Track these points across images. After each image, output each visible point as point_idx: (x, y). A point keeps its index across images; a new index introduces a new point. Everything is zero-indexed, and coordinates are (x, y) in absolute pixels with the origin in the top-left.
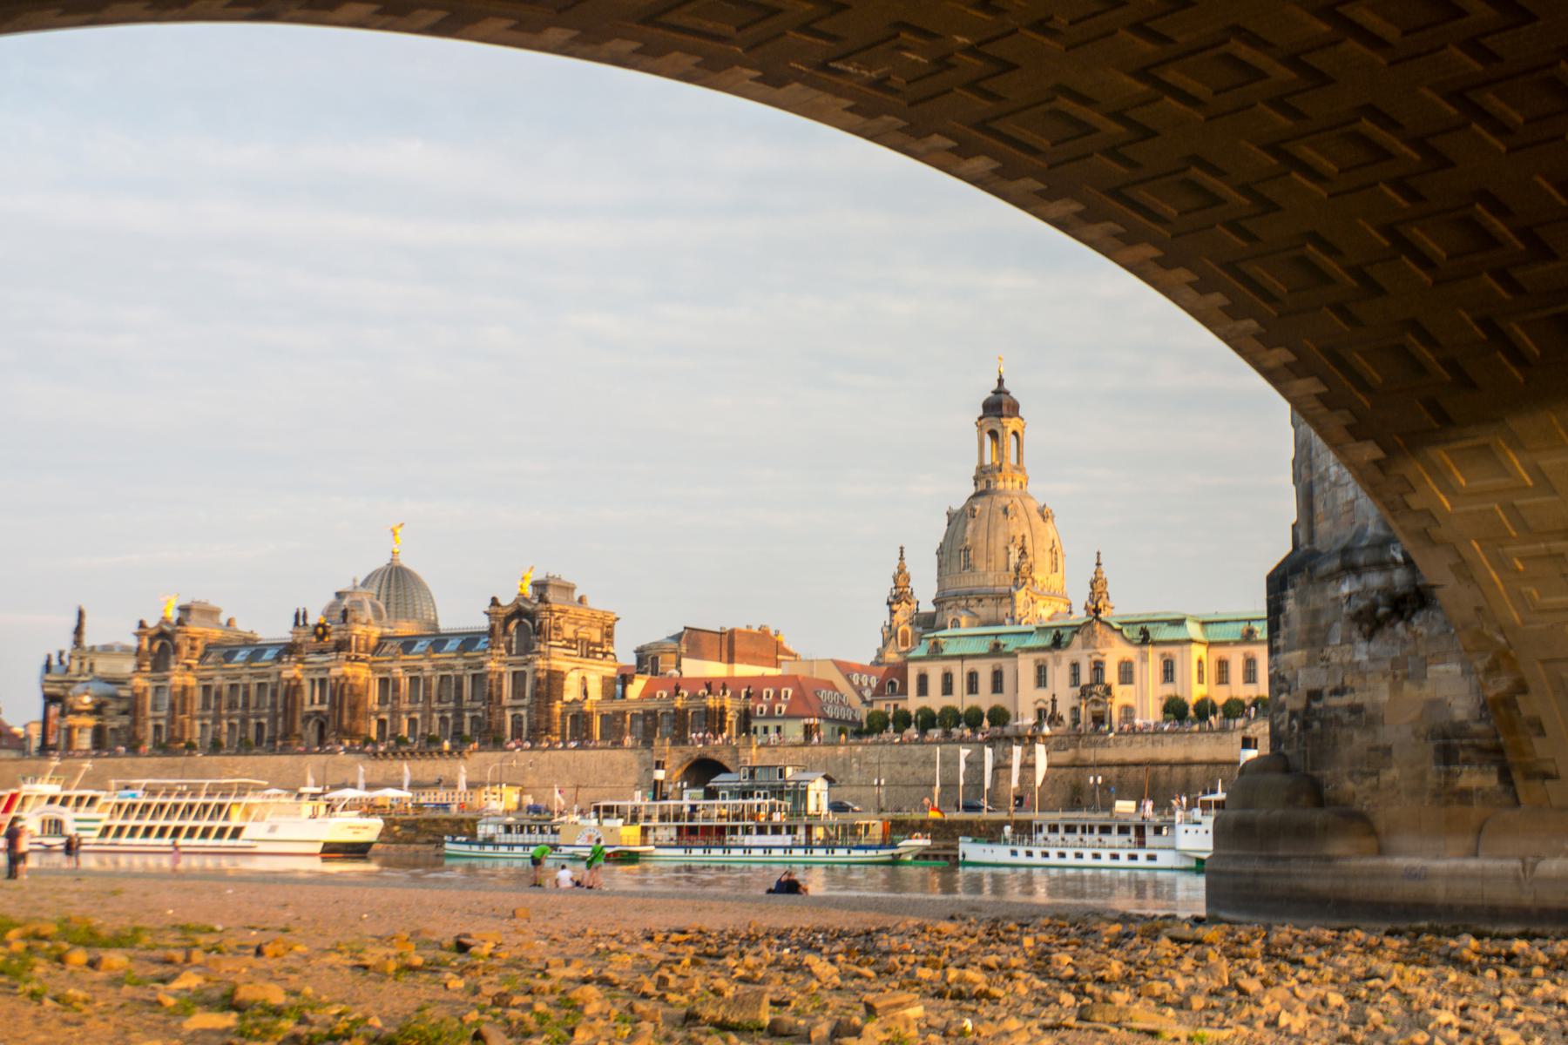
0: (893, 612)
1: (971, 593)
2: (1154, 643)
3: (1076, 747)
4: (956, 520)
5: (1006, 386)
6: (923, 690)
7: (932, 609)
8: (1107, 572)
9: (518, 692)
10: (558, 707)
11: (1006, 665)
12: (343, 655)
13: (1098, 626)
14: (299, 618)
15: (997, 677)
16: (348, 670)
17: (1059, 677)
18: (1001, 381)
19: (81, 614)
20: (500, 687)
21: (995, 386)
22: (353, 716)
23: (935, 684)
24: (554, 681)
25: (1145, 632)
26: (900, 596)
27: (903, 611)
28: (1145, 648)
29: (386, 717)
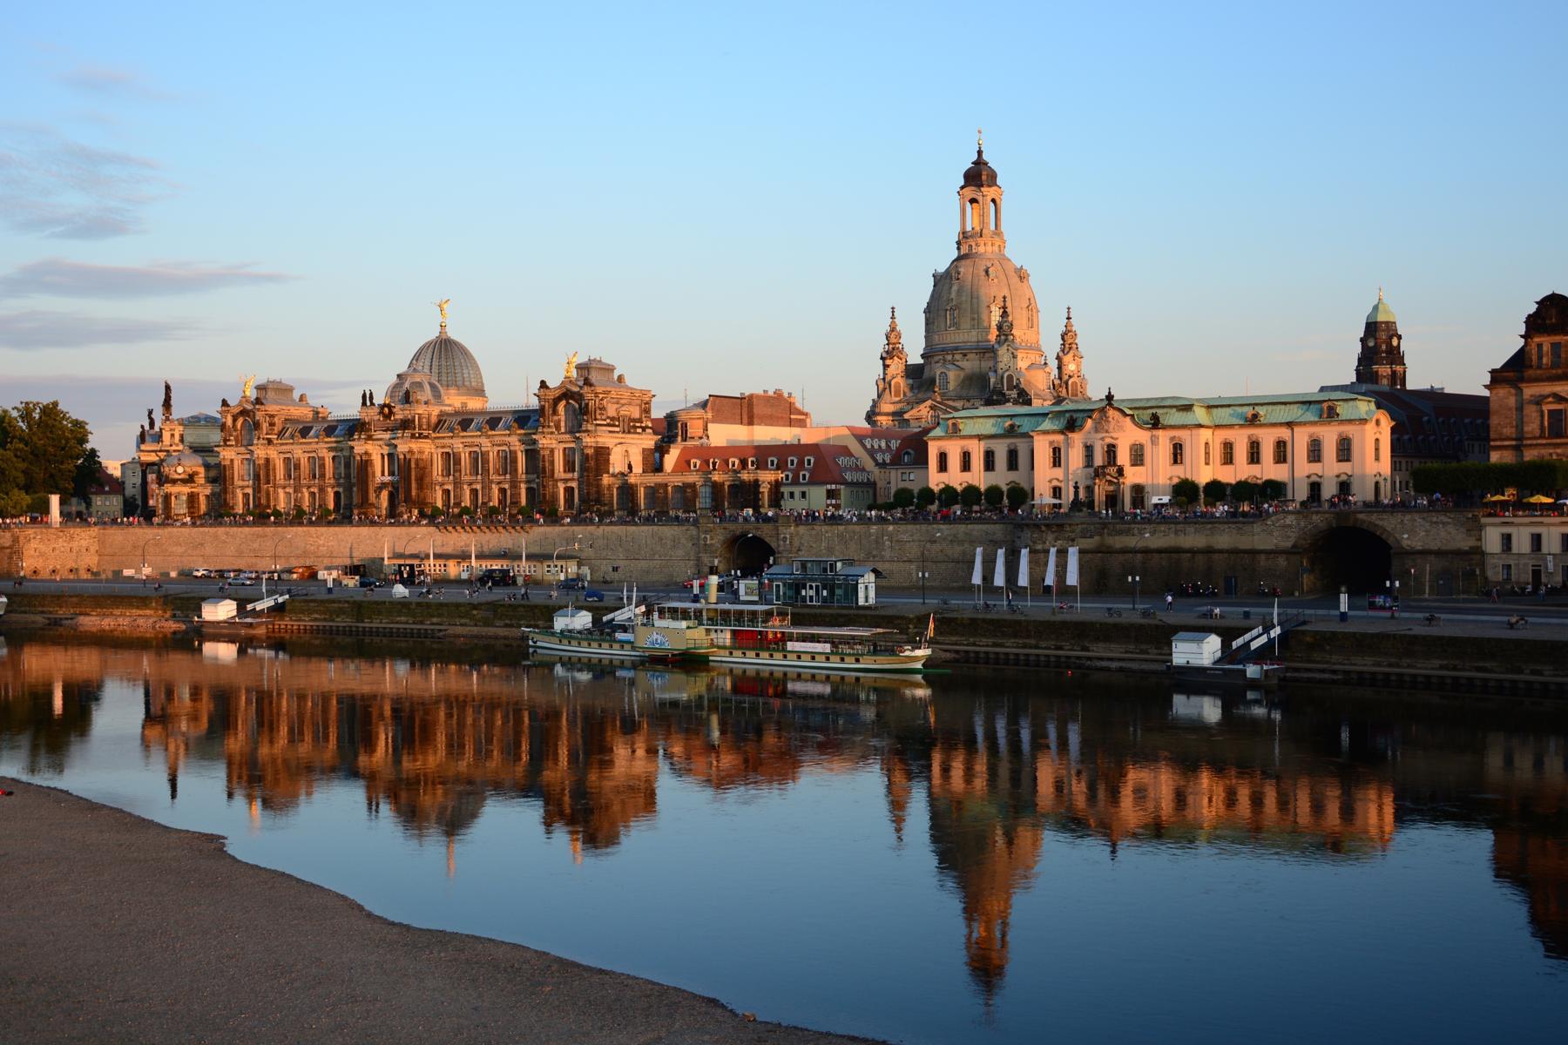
0: (886, 367)
1: (957, 349)
2: (1164, 428)
3: (1101, 535)
4: (941, 281)
5: (985, 157)
6: (943, 467)
7: (921, 361)
8: (1076, 325)
9: (569, 466)
10: (606, 480)
11: (1021, 446)
12: (408, 433)
13: (1111, 413)
14: (367, 399)
15: (1013, 456)
16: (415, 445)
17: (1075, 458)
18: (980, 153)
19: (168, 388)
20: (552, 463)
21: (975, 157)
22: (421, 487)
23: (954, 462)
24: (602, 454)
25: (1155, 418)
26: (892, 351)
27: (896, 367)
28: (1155, 432)
29: (450, 487)
